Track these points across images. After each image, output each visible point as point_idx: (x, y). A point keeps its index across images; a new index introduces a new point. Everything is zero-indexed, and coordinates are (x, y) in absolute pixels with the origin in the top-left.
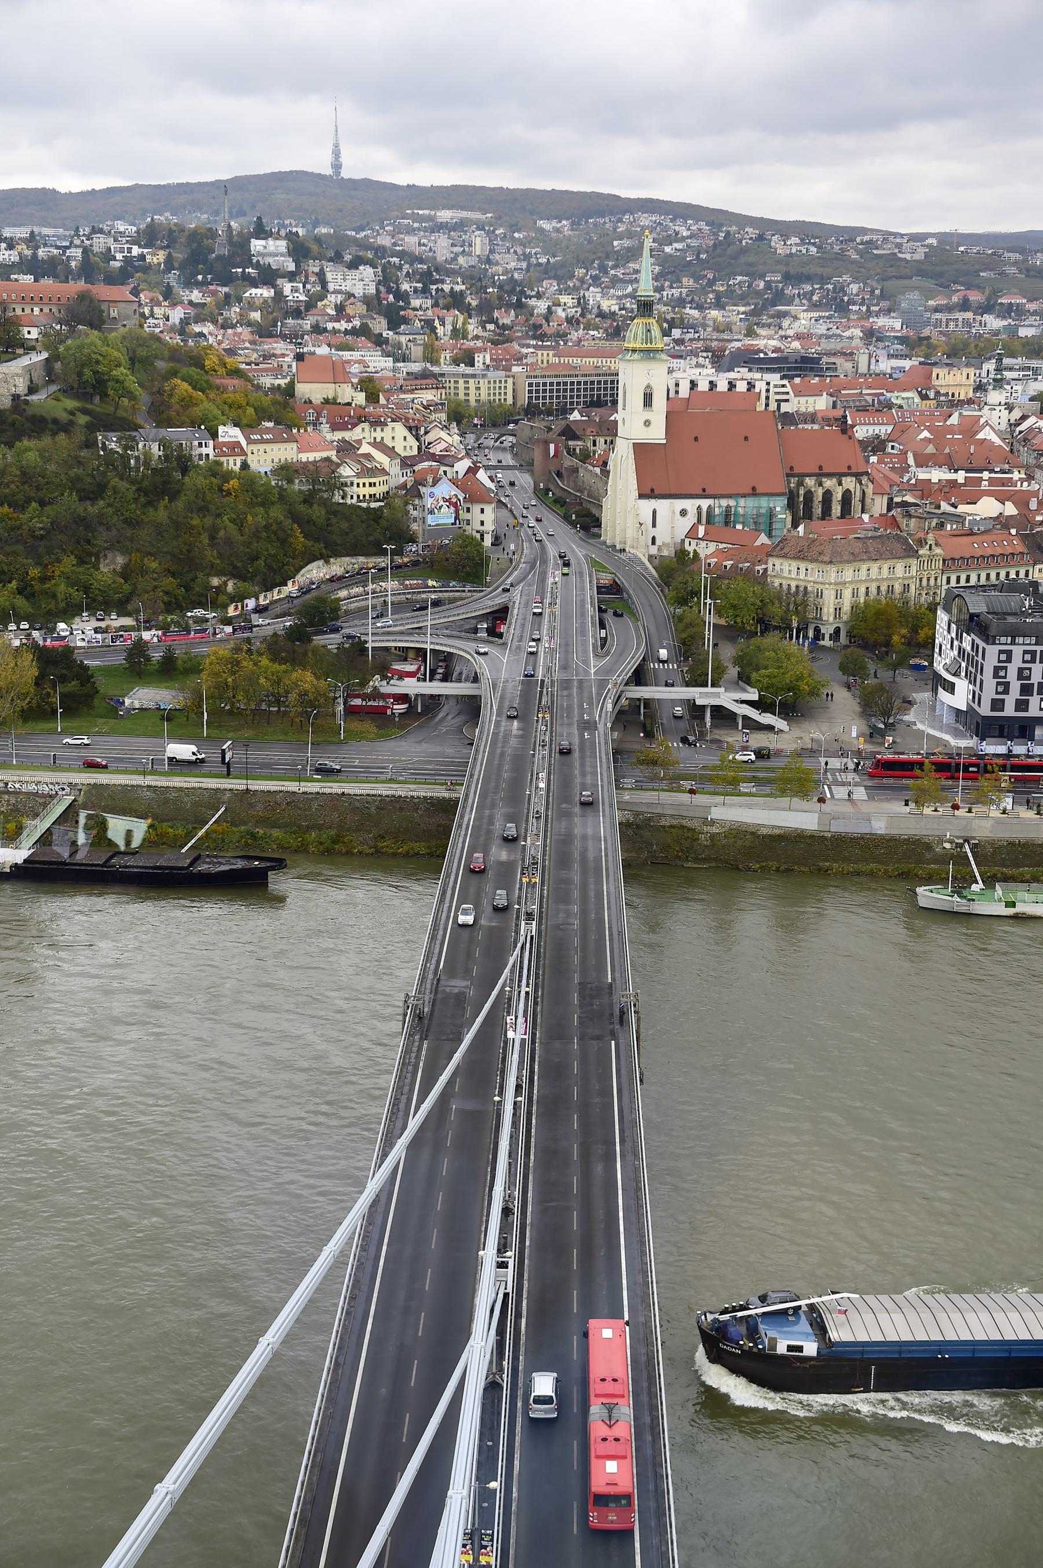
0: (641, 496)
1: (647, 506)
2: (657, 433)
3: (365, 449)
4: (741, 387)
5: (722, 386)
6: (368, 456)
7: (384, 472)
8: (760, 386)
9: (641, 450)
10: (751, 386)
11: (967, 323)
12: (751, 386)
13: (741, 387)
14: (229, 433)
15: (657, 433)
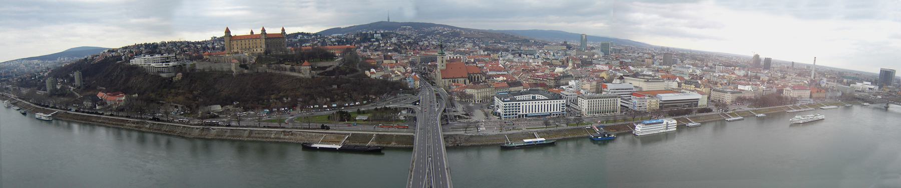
0: (443, 79)
1: (443, 80)
2: (444, 68)
3: (396, 72)
4: (458, 58)
5: (455, 58)
6: (397, 73)
7: (399, 76)
8: (462, 57)
9: (442, 71)
10: (460, 57)
11: (496, 46)
12: (460, 57)
13: (458, 58)
14: (373, 70)
15: (444, 68)
